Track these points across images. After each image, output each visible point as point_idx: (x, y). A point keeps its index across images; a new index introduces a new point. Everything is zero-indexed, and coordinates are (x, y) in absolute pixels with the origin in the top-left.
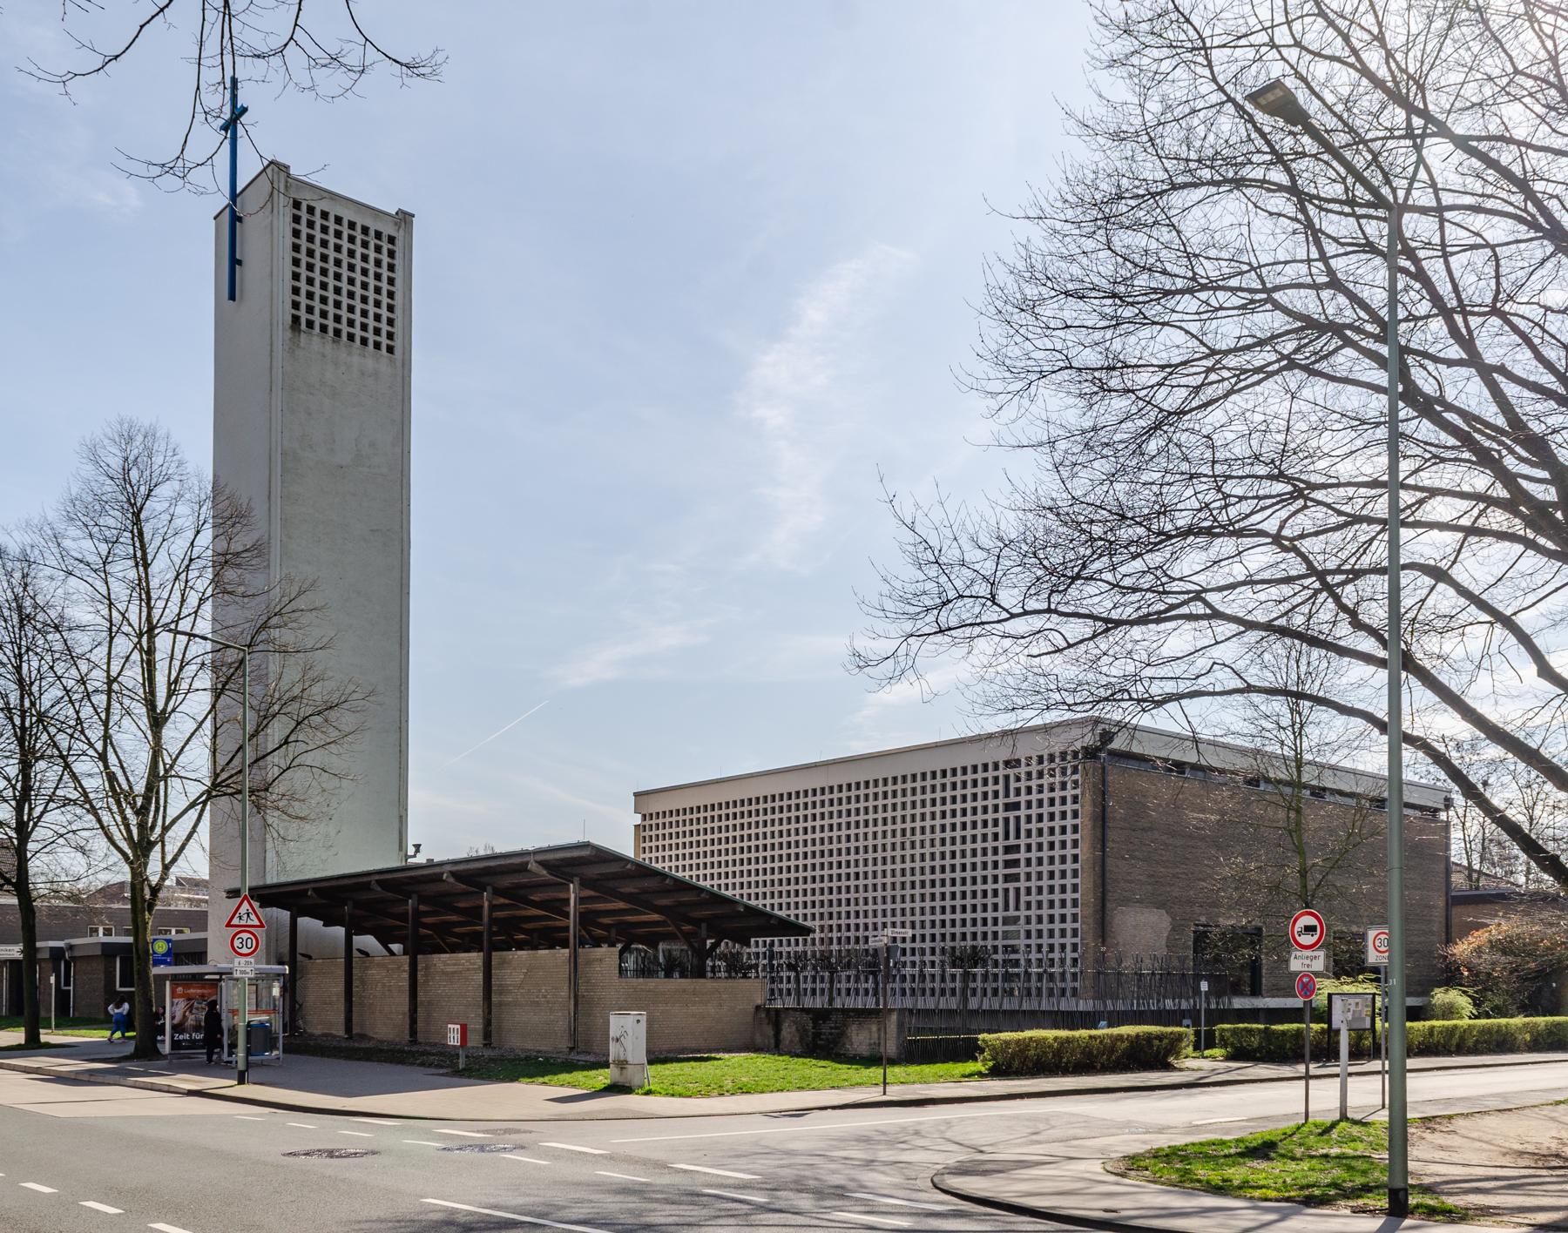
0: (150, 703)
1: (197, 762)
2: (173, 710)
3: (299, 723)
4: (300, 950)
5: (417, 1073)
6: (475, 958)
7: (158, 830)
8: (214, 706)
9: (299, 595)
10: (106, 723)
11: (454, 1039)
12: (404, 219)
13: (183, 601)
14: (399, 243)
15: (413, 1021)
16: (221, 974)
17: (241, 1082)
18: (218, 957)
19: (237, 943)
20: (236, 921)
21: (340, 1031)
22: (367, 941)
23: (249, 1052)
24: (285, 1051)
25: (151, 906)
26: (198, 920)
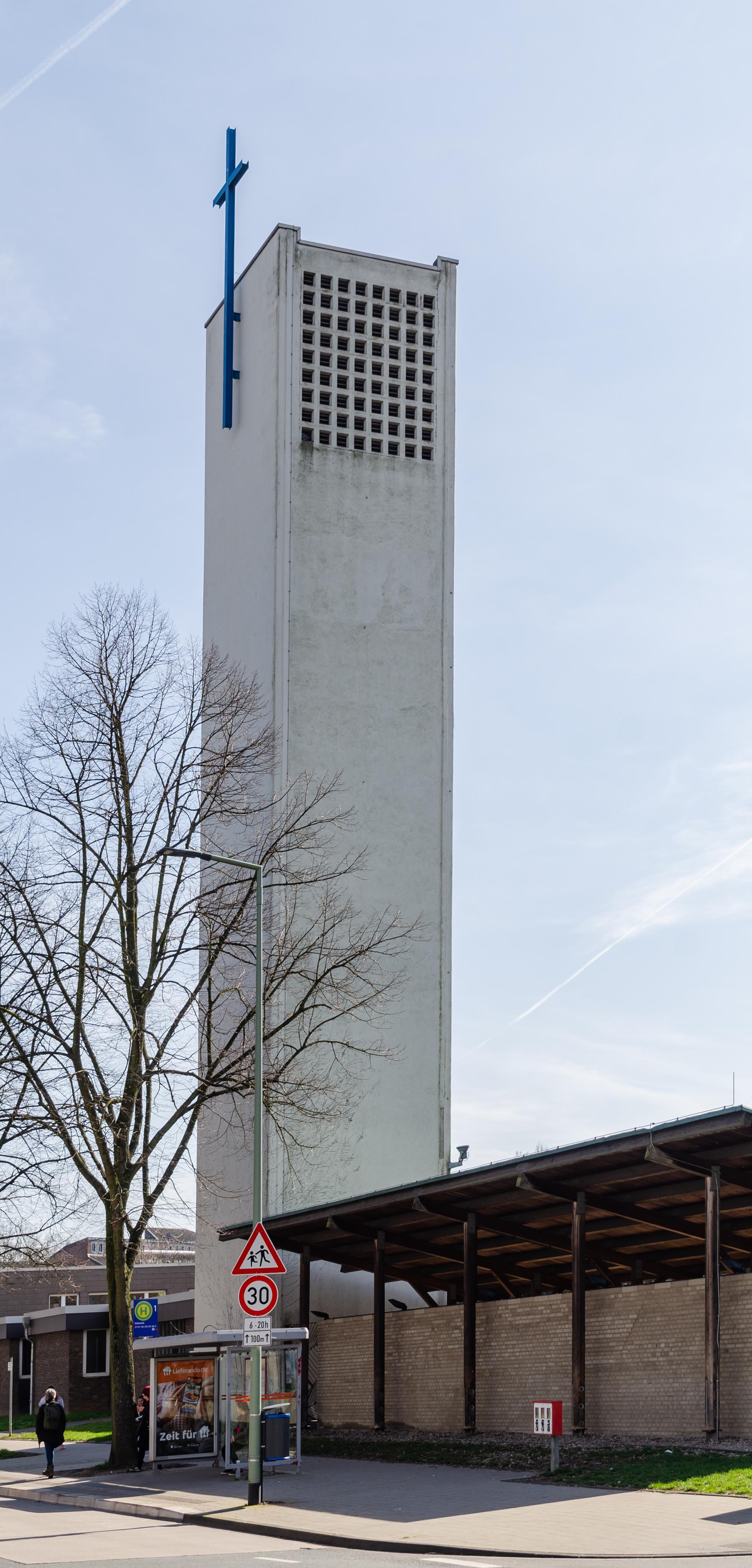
0: (131, 972)
1: (185, 1049)
2: (160, 980)
3: (318, 981)
4: (312, 1307)
5: (490, 1481)
6: (560, 1303)
7: (140, 1149)
8: (206, 976)
9: (317, 800)
10: (77, 1011)
11: (542, 1423)
12: (445, 268)
13: (172, 827)
14: (438, 304)
15: (470, 1400)
16: (218, 1345)
17: (253, 1501)
18: (208, 1324)
19: (248, 1296)
20: (246, 1265)
21: (367, 1419)
22: (400, 1289)
23: (263, 1456)
24: (304, 1452)
25: (132, 1254)
26: (183, 1277)
